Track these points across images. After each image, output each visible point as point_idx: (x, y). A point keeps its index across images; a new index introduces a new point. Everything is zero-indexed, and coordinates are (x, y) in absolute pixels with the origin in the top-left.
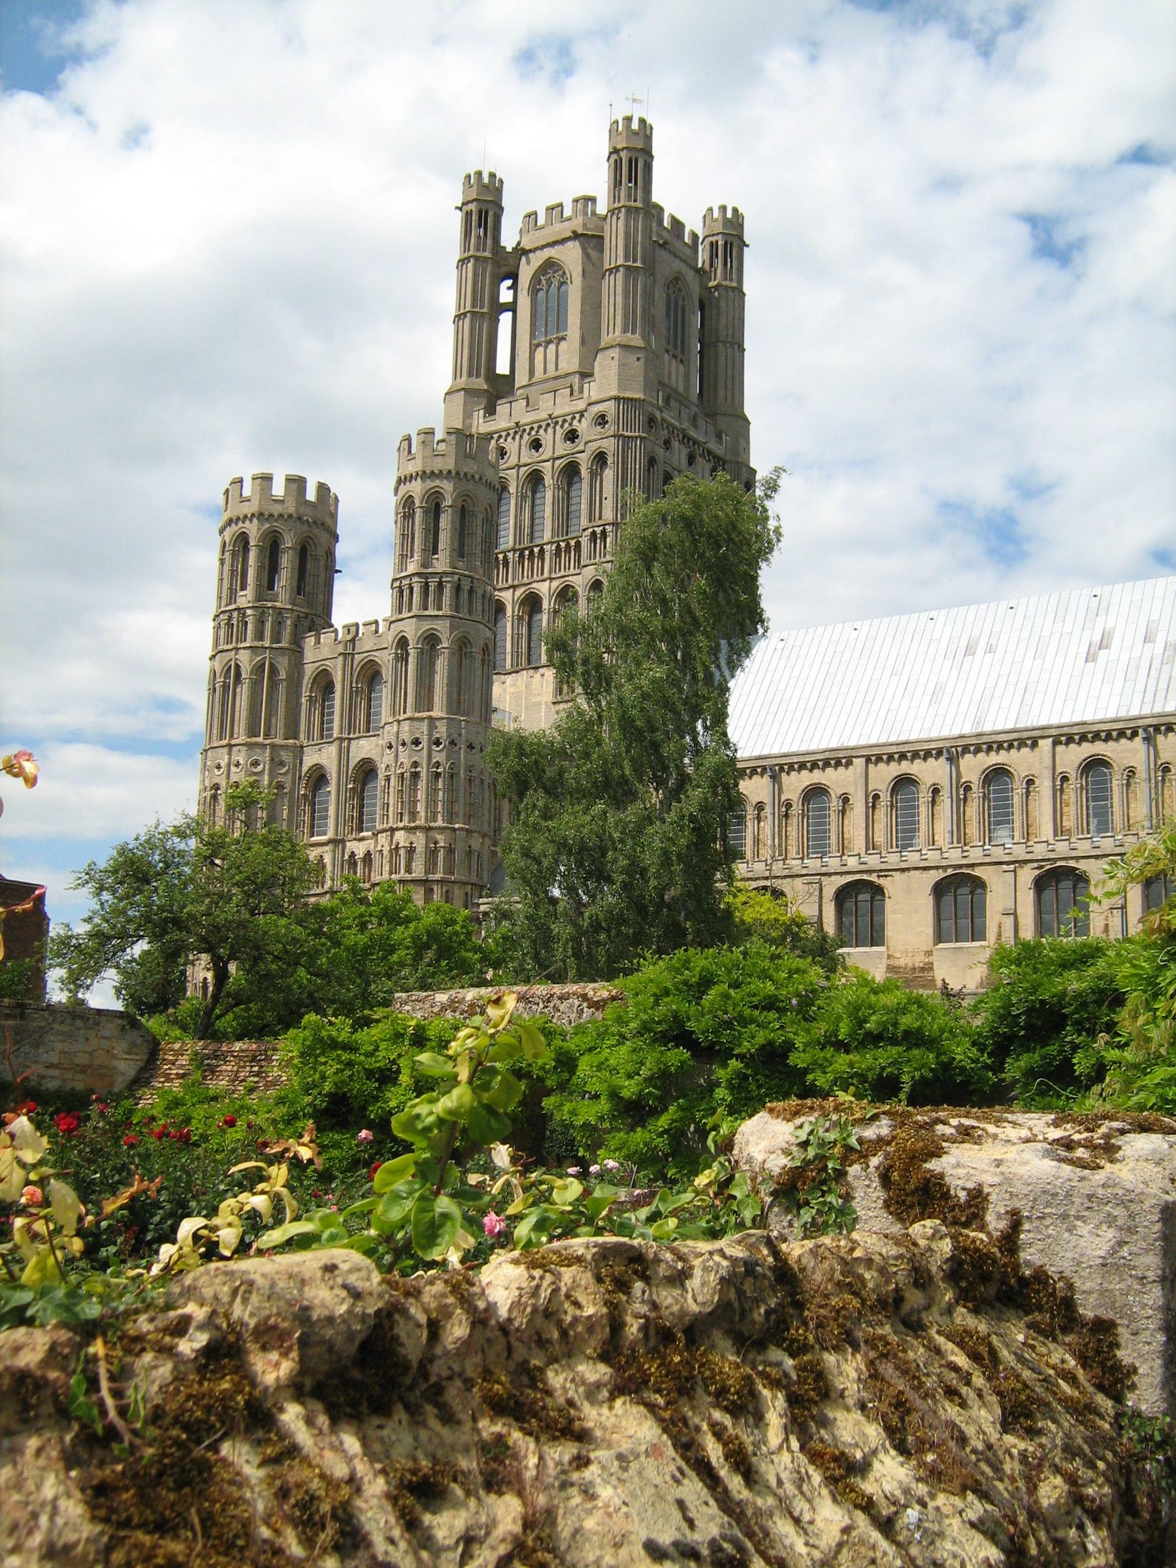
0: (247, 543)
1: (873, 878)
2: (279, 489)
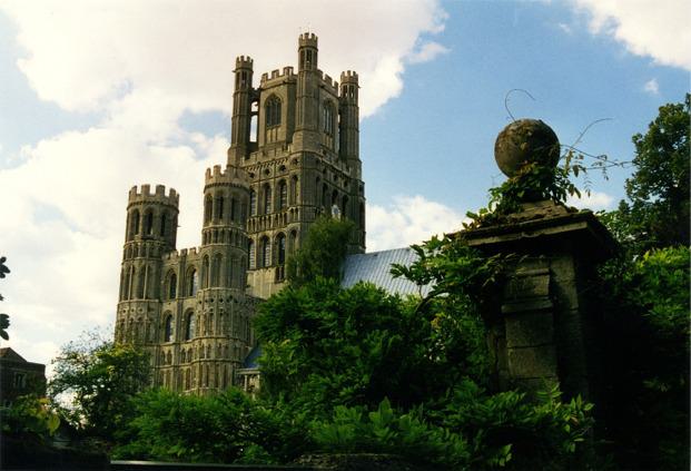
2: (153, 191)
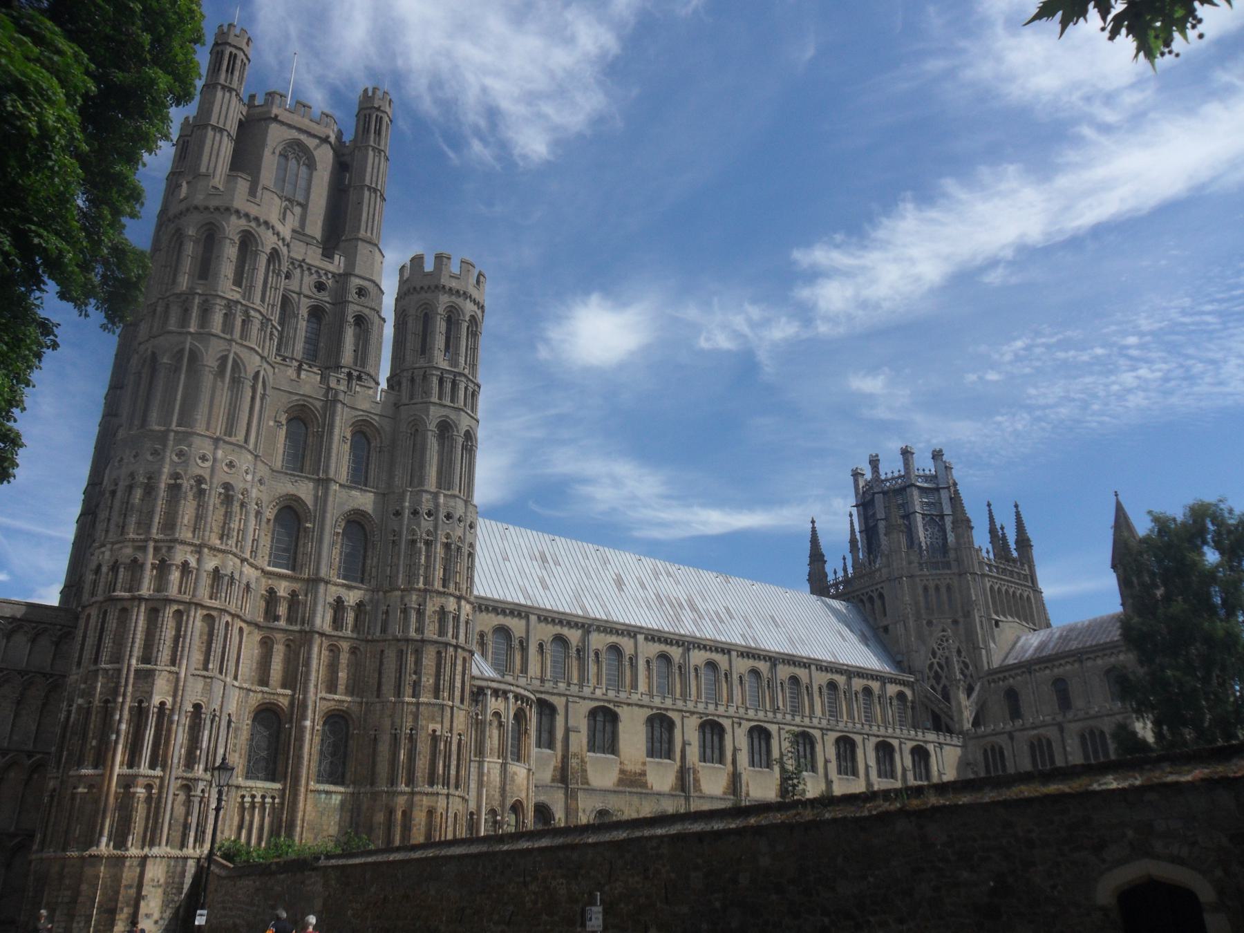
1: (611, 706)
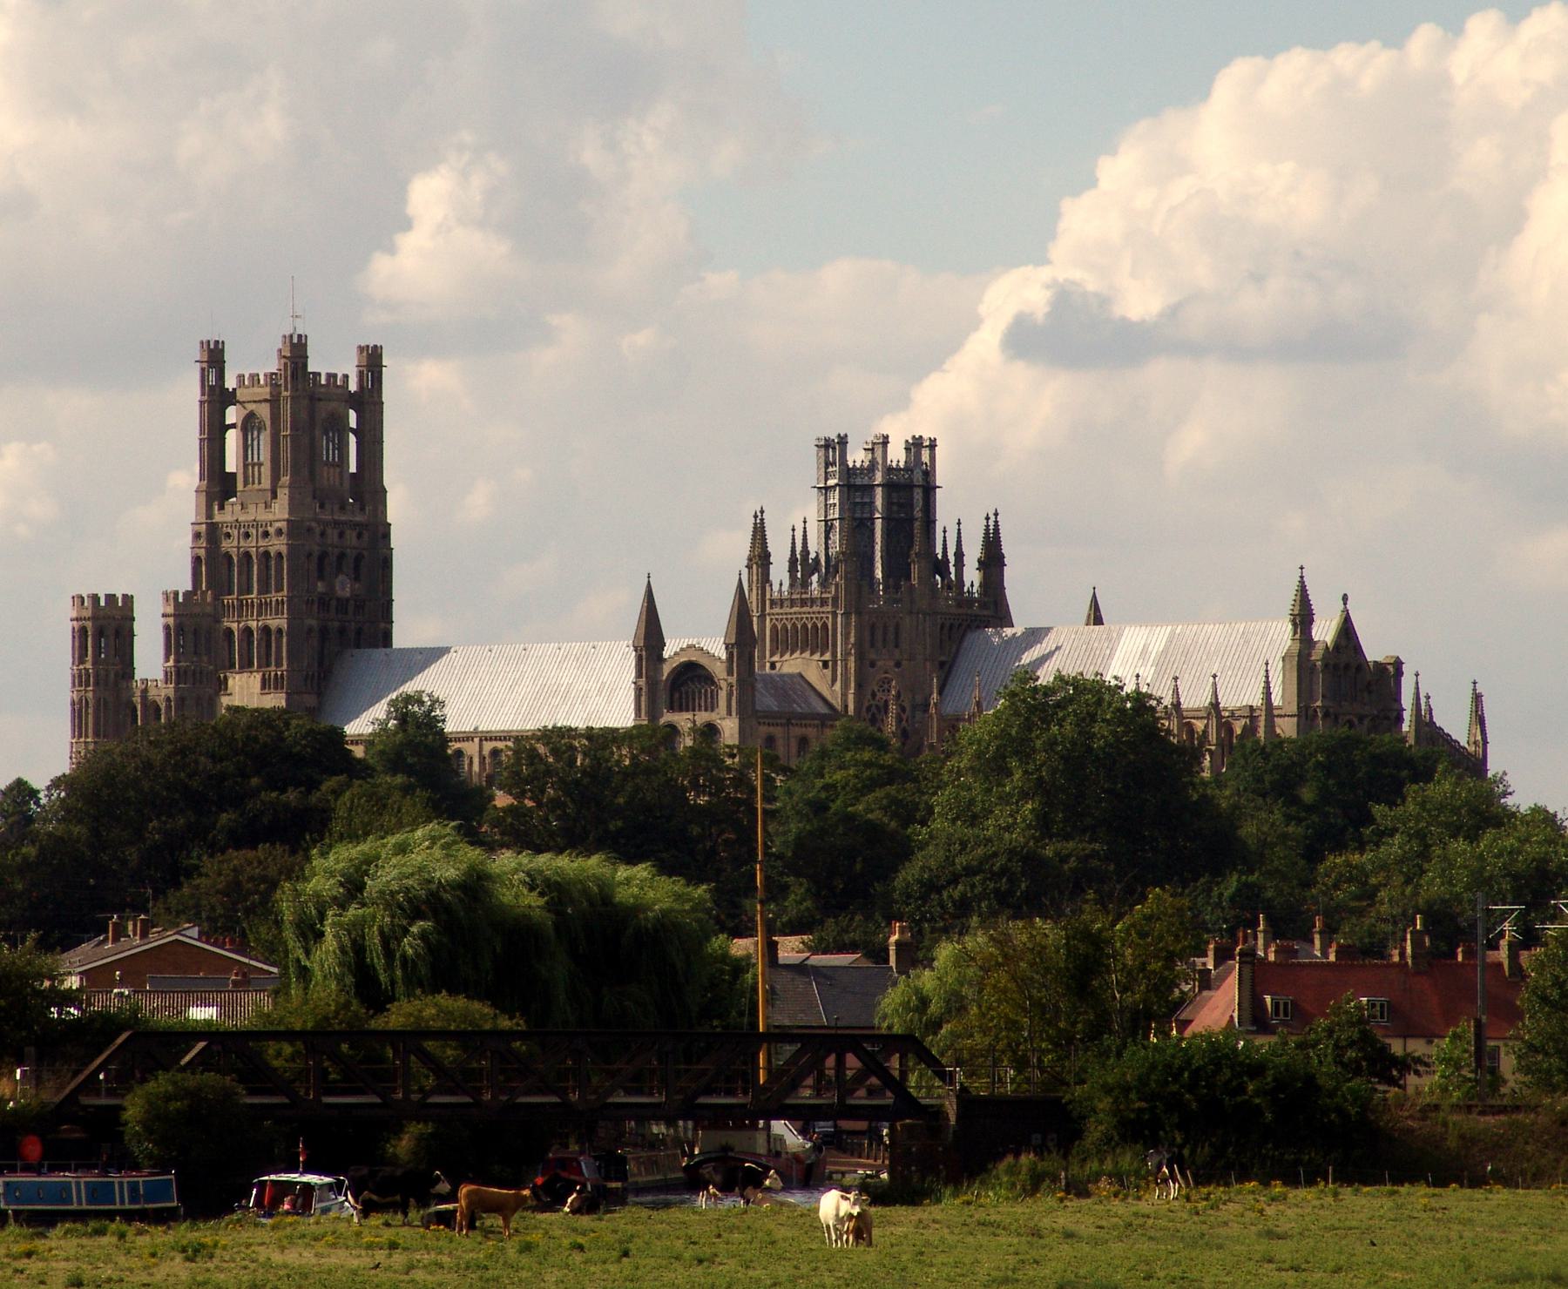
0: (87, 632)
